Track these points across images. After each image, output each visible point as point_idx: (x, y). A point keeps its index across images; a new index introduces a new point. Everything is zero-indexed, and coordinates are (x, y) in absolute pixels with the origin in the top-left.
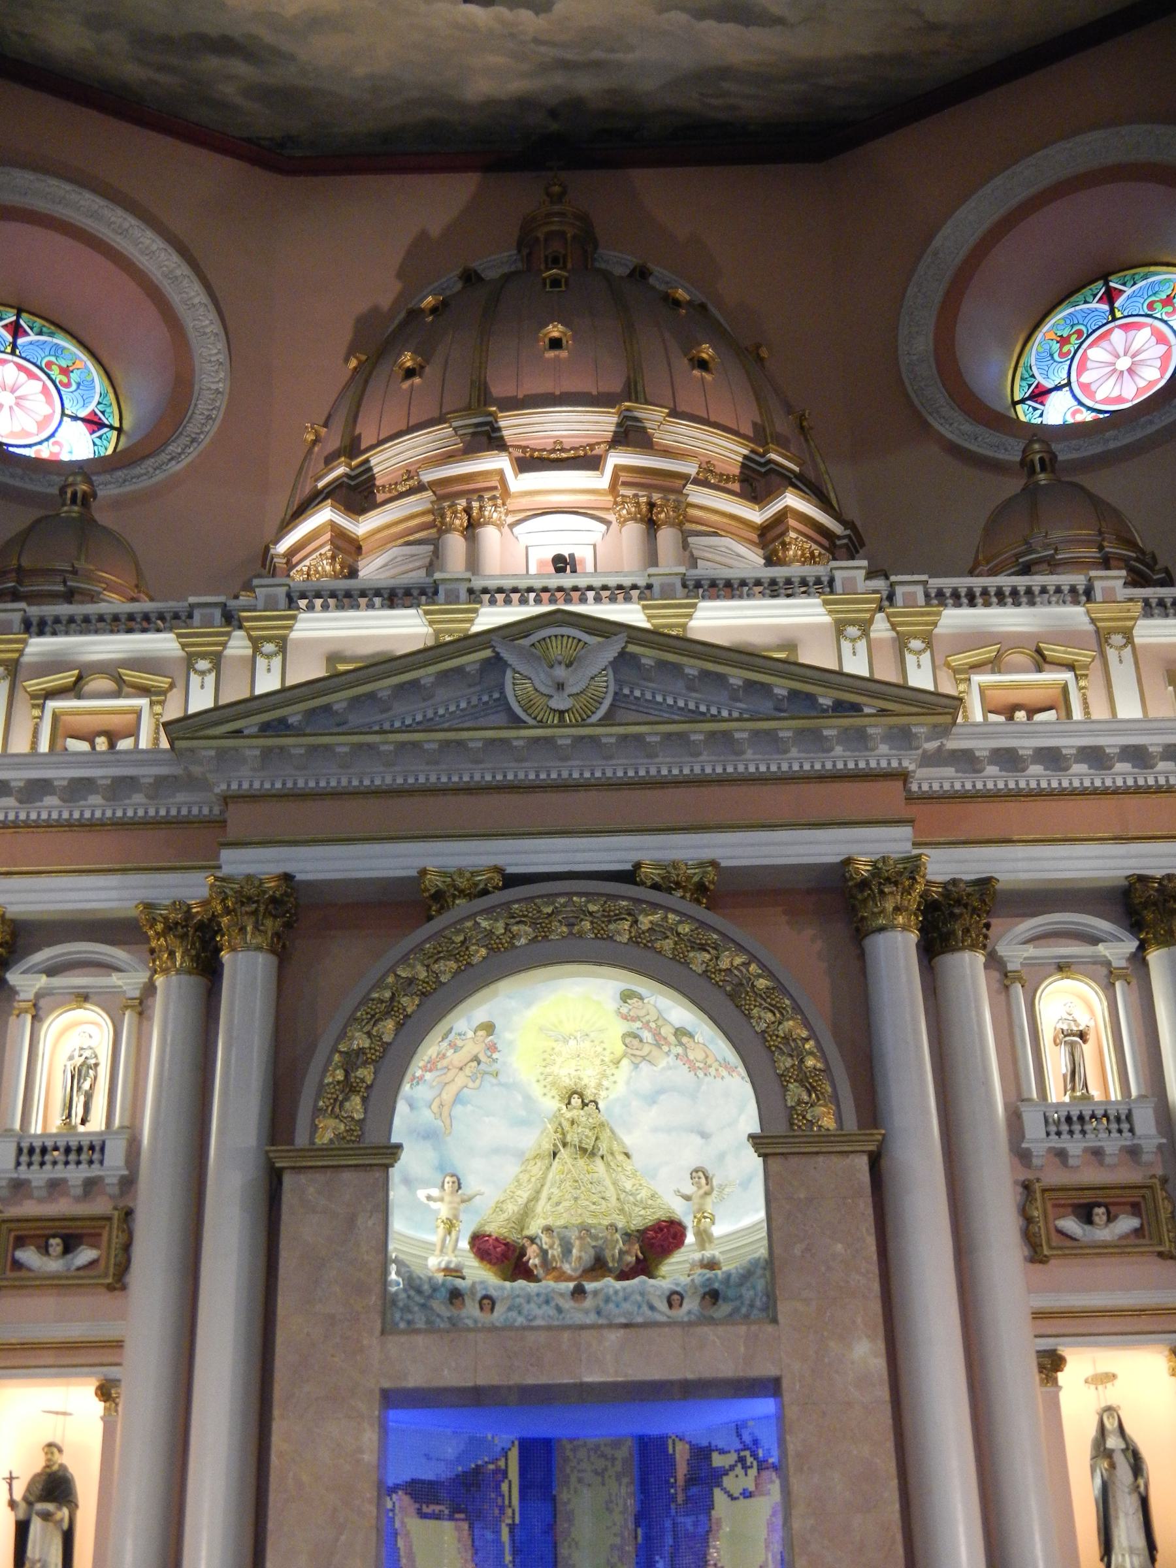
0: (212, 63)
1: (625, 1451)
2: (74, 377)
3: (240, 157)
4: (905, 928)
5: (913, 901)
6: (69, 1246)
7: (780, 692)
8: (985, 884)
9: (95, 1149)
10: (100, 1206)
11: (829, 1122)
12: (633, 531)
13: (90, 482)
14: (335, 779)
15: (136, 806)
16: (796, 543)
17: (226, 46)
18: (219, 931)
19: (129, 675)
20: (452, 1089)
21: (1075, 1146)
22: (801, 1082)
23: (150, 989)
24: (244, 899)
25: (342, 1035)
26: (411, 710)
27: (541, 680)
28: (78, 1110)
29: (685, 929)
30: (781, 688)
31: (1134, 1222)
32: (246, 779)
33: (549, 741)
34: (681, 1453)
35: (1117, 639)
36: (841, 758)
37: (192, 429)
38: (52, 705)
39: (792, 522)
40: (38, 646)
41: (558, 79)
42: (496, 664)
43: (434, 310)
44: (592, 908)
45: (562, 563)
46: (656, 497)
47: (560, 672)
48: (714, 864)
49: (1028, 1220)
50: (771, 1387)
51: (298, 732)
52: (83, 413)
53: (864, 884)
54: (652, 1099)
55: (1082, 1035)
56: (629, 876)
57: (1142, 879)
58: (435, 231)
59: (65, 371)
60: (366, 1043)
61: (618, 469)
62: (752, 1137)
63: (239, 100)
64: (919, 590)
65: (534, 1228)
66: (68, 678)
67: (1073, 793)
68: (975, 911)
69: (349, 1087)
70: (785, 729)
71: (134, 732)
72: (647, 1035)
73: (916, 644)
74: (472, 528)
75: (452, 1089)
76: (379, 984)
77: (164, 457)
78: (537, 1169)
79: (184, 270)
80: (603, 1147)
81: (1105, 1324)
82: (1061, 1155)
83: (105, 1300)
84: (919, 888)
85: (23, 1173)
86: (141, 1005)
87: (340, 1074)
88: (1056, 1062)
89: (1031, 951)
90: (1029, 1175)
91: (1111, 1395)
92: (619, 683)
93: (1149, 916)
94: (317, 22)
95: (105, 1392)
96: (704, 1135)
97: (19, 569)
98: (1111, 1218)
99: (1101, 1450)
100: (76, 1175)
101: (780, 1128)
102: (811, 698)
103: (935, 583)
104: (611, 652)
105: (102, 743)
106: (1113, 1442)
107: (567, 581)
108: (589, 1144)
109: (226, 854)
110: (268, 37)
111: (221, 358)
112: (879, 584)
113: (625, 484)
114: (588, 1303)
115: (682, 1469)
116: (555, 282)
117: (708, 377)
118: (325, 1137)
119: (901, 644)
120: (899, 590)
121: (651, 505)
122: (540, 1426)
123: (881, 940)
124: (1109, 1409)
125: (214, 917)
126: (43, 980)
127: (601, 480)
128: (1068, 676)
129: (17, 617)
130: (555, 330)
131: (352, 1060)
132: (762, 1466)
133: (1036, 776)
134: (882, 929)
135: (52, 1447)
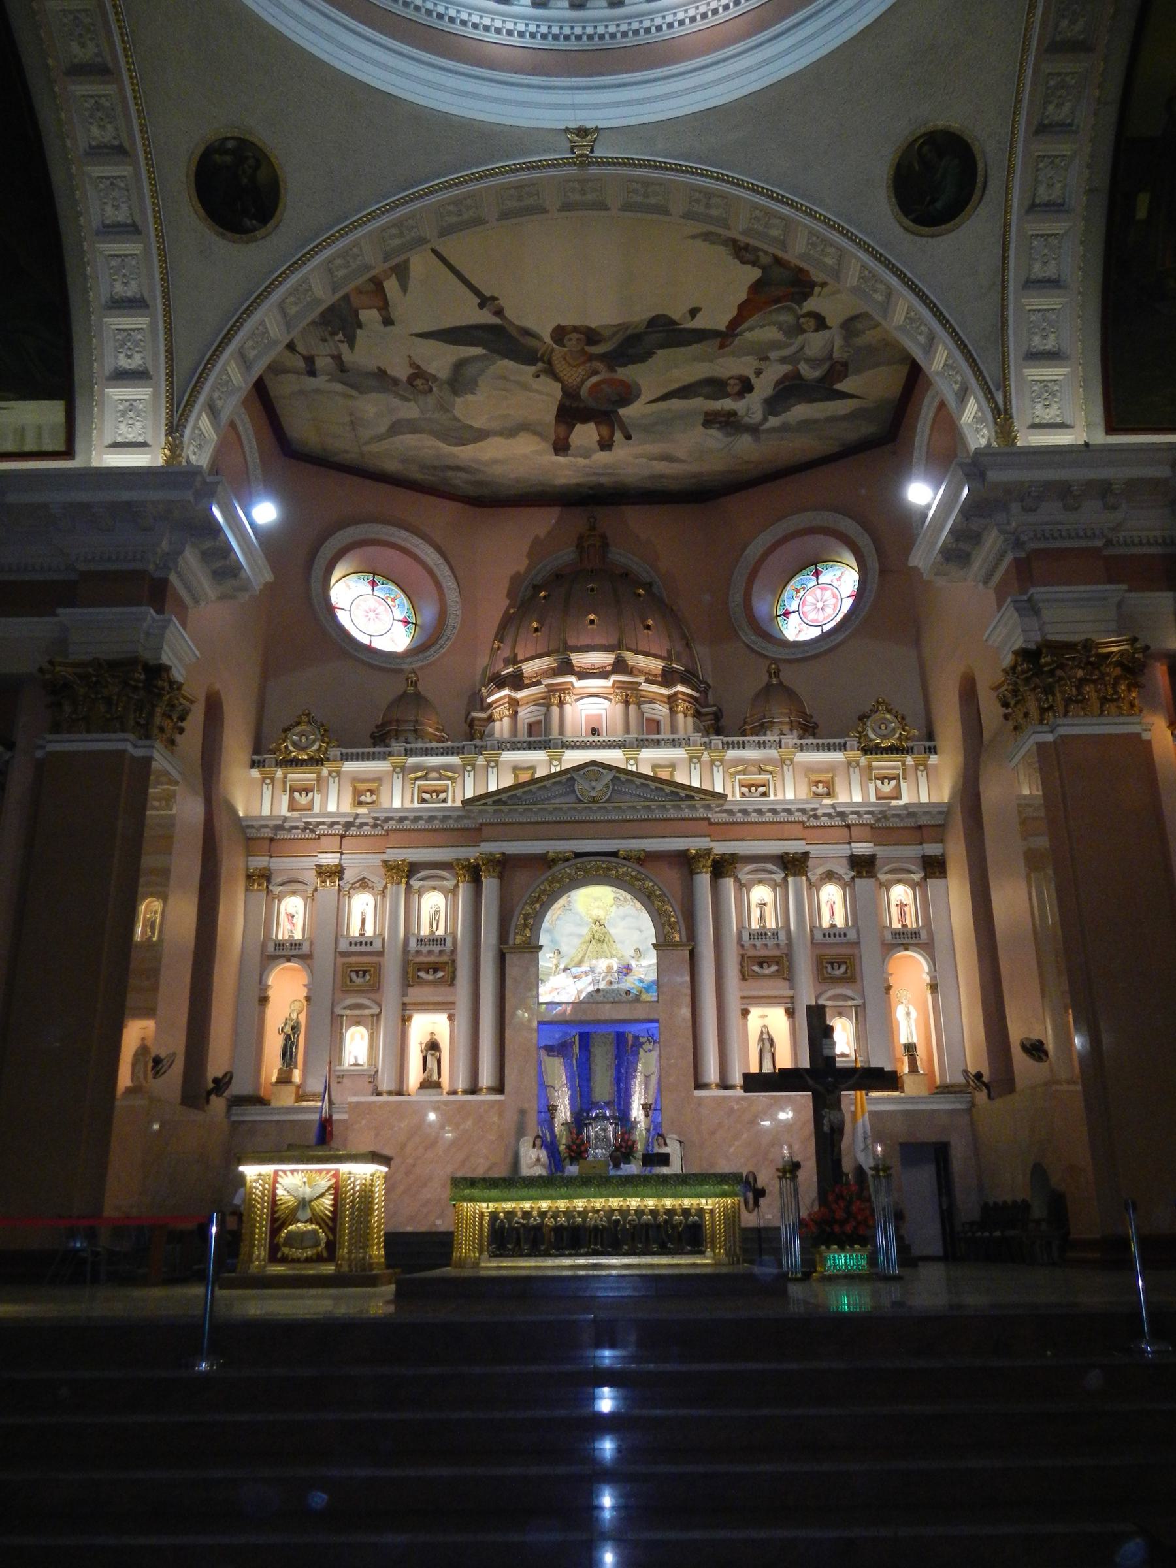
0: (450, 474)
1: (613, 1036)
2: (397, 602)
3: (462, 502)
4: (706, 872)
5: (709, 863)
6: (435, 972)
7: (668, 791)
8: (734, 855)
9: (443, 940)
10: (444, 959)
11: (677, 939)
12: (620, 707)
13: (416, 675)
14: (517, 818)
15: (451, 824)
16: (681, 706)
17: (458, 468)
18: (481, 870)
19: (443, 772)
20: (556, 915)
21: (758, 943)
22: (669, 925)
23: (457, 886)
24: (489, 861)
25: (523, 909)
26: (543, 794)
27: (587, 786)
28: (435, 926)
29: (634, 873)
31: (777, 968)
32: (488, 818)
33: (590, 808)
34: (630, 1038)
35: (788, 762)
36: (687, 813)
37: (447, 632)
38: (417, 783)
39: (680, 696)
40: (412, 760)
41: (594, 479)
42: (572, 779)
43: (545, 597)
44: (604, 866)
45: (594, 731)
46: (629, 692)
47: (594, 784)
48: (644, 850)
49: (742, 967)
50: (657, 1021)
51: (505, 803)
52: (401, 618)
53: (693, 858)
54: (623, 918)
55: (765, 904)
56: (614, 854)
57: (787, 854)
59: (393, 600)
60: (531, 911)
61: (615, 682)
62: (653, 945)
63: (461, 484)
64: (720, 742)
66: (424, 773)
67: (767, 823)
68: (731, 864)
69: (525, 926)
70: (669, 805)
72: (622, 898)
73: (718, 763)
74: (561, 704)
75: (556, 915)
76: (534, 892)
77: (438, 646)
78: (584, 947)
79: (441, 561)
80: (606, 940)
81: (764, 1000)
82: (754, 946)
83: (448, 989)
84: (712, 857)
85: (420, 948)
86: (454, 891)
87: (523, 922)
88: (755, 913)
89: (750, 876)
90: (743, 952)
91: (766, 1021)
92: (614, 785)
93: (789, 866)
94: (495, 462)
95: (451, 1018)
96: (641, 931)
97: (397, 721)
98: (769, 966)
99: (761, 1039)
100: (437, 949)
101: (662, 940)
102: (677, 794)
103: (726, 739)
104: (610, 777)
105: (434, 795)
106: (765, 1036)
107: (596, 739)
108: (602, 939)
109: (482, 844)
110: (474, 465)
111: (457, 599)
112: (706, 739)
113: (618, 688)
114: (601, 994)
115: (630, 1043)
116: (592, 590)
117: (650, 632)
118: (518, 942)
119: (712, 762)
120: (713, 742)
121: (627, 695)
122: (586, 1029)
123: (698, 876)
124: (765, 1026)
125: (478, 865)
126: (421, 883)
127: (607, 683)
128: (769, 776)
129: (403, 749)
130: (592, 617)
132: (655, 1042)
133: (754, 817)
134: (698, 873)
135: (432, 1034)
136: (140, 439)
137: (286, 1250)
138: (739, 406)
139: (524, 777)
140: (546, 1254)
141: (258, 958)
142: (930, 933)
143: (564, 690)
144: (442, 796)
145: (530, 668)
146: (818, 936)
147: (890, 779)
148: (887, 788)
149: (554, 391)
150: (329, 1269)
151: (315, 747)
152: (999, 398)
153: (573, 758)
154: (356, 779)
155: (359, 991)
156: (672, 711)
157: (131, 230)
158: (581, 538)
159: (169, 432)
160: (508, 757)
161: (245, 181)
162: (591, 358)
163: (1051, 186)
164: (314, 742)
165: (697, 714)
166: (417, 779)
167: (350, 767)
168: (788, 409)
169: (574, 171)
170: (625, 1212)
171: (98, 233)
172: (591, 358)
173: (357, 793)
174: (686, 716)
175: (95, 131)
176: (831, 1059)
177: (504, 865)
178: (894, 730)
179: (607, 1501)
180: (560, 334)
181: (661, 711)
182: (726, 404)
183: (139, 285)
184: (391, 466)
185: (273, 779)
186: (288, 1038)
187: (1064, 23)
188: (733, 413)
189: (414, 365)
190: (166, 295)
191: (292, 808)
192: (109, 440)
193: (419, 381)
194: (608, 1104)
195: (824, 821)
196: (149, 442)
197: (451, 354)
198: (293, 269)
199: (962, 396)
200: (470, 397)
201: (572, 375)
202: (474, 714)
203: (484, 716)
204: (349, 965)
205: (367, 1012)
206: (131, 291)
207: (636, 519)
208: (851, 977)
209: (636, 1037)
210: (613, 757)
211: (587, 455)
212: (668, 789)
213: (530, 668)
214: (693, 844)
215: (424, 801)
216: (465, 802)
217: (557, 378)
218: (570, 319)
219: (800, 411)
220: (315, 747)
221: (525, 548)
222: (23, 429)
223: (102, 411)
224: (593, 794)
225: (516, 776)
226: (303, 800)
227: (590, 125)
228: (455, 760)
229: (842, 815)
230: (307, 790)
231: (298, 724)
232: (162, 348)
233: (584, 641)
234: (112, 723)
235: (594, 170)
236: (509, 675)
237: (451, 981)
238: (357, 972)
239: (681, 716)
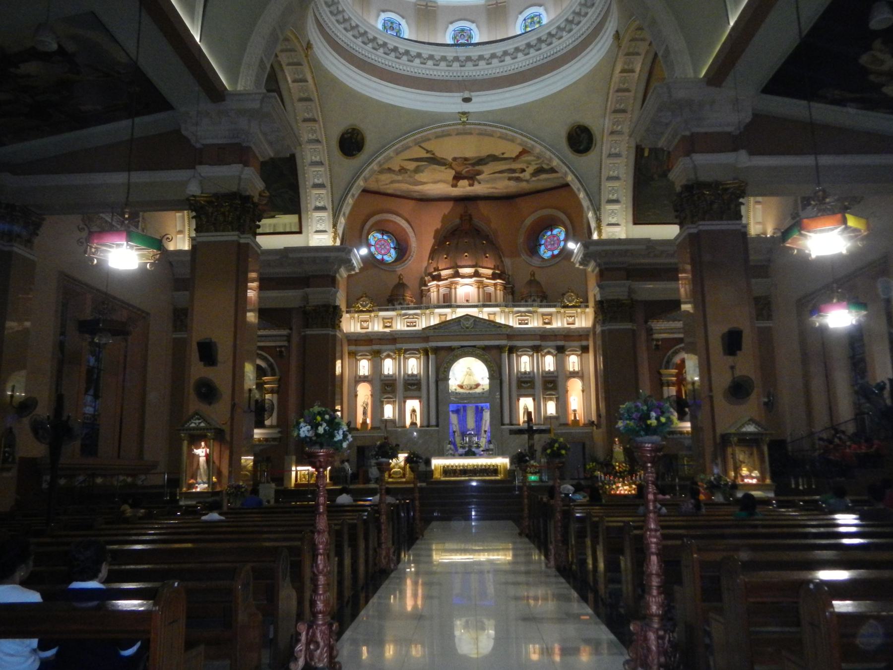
9: (416, 376)
12: (476, 290)
17: (415, 192)
27: (465, 323)
30: (493, 324)
34: (480, 407)
40: (403, 312)
42: (459, 321)
43: (449, 244)
56: (474, 346)
58: (446, 213)
65: (464, 384)
69: (445, 371)
71: (415, 322)
74: (455, 288)
95: (420, 402)
99: (524, 408)
104: (472, 321)
131: (445, 368)
136: (324, 229)
137: (393, 475)
138: (521, 175)
139: (443, 319)
140: (458, 477)
141: (353, 381)
142: (583, 374)
143: (457, 283)
144: (414, 324)
145: (444, 273)
146: (544, 374)
147: (572, 317)
148: (571, 320)
149: (453, 172)
150: (404, 480)
151: (369, 306)
152: (598, 213)
153: (461, 312)
154: (384, 319)
155: (389, 393)
156: (495, 289)
157: (321, 163)
158: (461, 215)
159: (333, 228)
160: (437, 311)
161: (354, 141)
162: (466, 164)
163: (615, 149)
164: (368, 304)
165: (505, 288)
166: (406, 318)
167: (382, 314)
168: (539, 176)
169: (461, 126)
171: (310, 165)
172: (466, 164)
173: (384, 323)
174: (500, 290)
175: (310, 135)
176: (532, 427)
177: (436, 350)
178: (574, 300)
179: (473, 513)
180: (455, 159)
181: (491, 289)
182: (517, 175)
183: (323, 180)
184: (389, 191)
185: (354, 317)
186: (365, 408)
187: (618, 105)
188: (519, 177)
189: (400, 166)
190: (331, 183)
191: (362, 328)
192: (314, 230)
194: (473, 430)
196: (327, 230)
197: (415, 164)
198: (368, 166)
199: (588, 209)
200: (421, 174)
201: (459, 169)
202: (423, 288)
203: (426, 288)
204: (385, 384)
205: (391, 400)
206: (320, 181)
207: (481, 205)
208: (555, 388)
209: (482, 407)
210: (473, 312)
211: (464, 187)
212: (493, 324)
213: (444, 273)
215: (408, 326)
216: (423, 329)
217: (453, 169)
218: (456, 155)
219: (544, 176)
220: (369, 306)
221: (440, 219)
222: (285, 224)
223: (312, 220)
224: (467, 326)
225: (440, 318)
226: (365, 325)
227: (467, 111)
228: (418, 311)
230: (366, 321)
231: (362, 297)
232: (330, 200)
233: (463, 263)
234: (324, 325)
235: (468, 126)
236: (436, 275)
237: (419, 389)
238: (388, 386)
239: (498, 291)
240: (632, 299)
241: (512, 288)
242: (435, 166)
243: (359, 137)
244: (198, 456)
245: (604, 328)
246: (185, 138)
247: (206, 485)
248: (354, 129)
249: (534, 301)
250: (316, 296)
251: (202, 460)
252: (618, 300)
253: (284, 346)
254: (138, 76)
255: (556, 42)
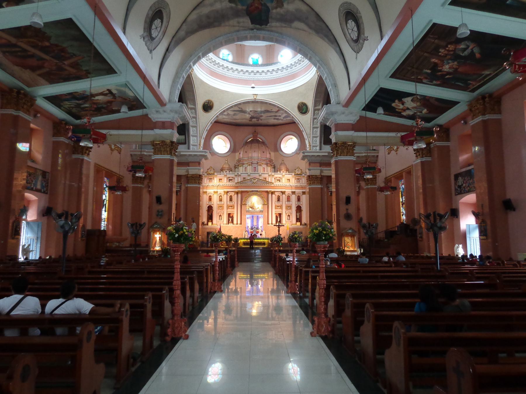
15: (233, 186)
36: (268, 185)
56: (257, 191)
138: (279, 118)
149: (250, 116)
152: (309, 139)
170: (257, 241)
177: (242, 192)
180: (251, 111)
193: (228, 114)
195: (288, 186)
201: (252, 115)
214: (268, 190)
227: (256, 94)
229: (291, 185)
234: (195, 183)
240: (322, 176)
241: (274, 165)
242: (242, 113)
243: (211, 104)
244: (156, 238)
245: (310, 187)
246: (149, 117)
247: (160, 248)
248: (209, 100)
249: (283, 172)
250: (192, 171)
251: (158, 239)
252: (316, 176)
253: (179, 191)
254: (136, 99)
255: (294, 68)
